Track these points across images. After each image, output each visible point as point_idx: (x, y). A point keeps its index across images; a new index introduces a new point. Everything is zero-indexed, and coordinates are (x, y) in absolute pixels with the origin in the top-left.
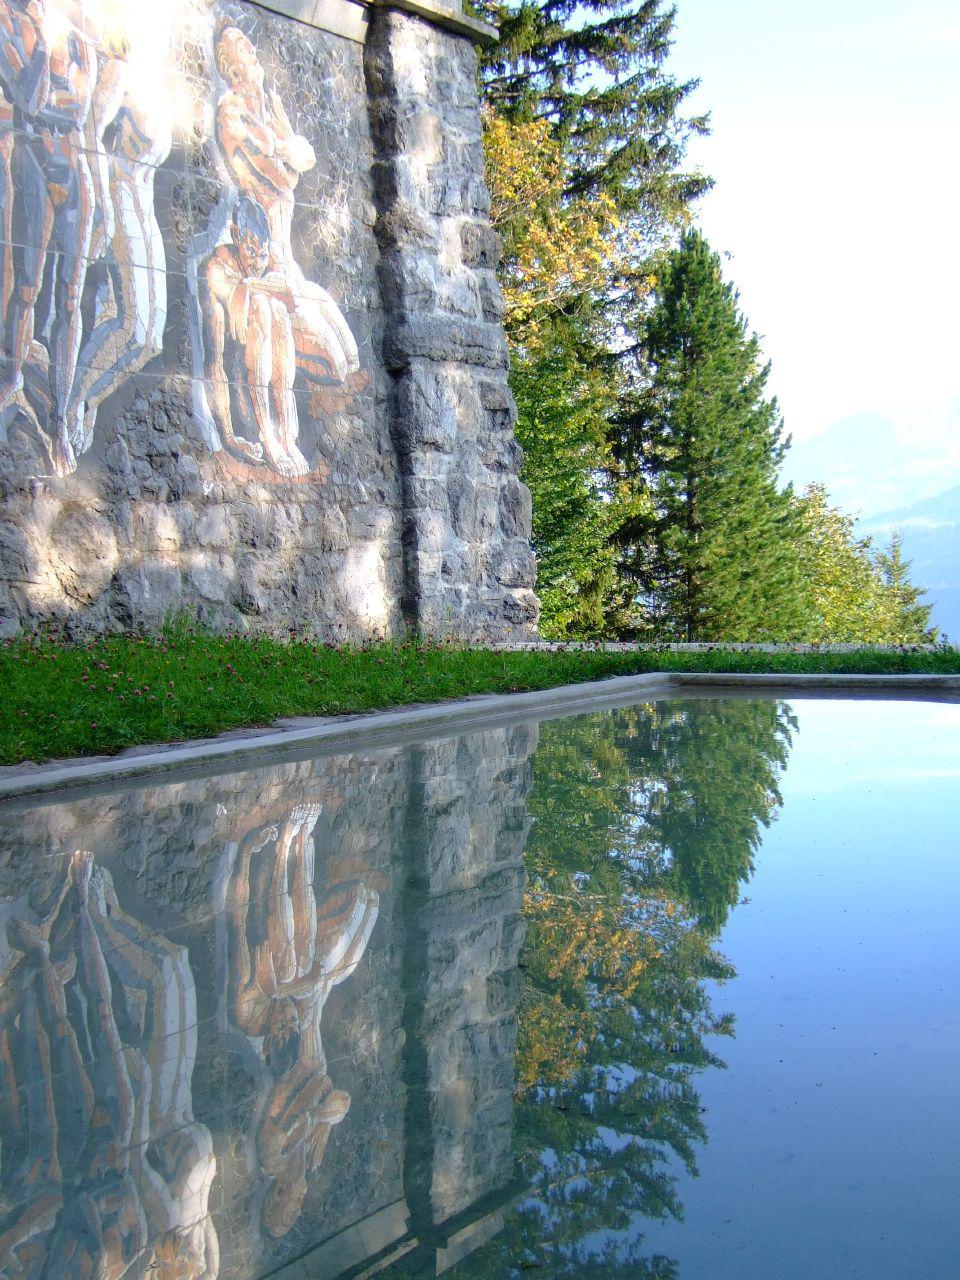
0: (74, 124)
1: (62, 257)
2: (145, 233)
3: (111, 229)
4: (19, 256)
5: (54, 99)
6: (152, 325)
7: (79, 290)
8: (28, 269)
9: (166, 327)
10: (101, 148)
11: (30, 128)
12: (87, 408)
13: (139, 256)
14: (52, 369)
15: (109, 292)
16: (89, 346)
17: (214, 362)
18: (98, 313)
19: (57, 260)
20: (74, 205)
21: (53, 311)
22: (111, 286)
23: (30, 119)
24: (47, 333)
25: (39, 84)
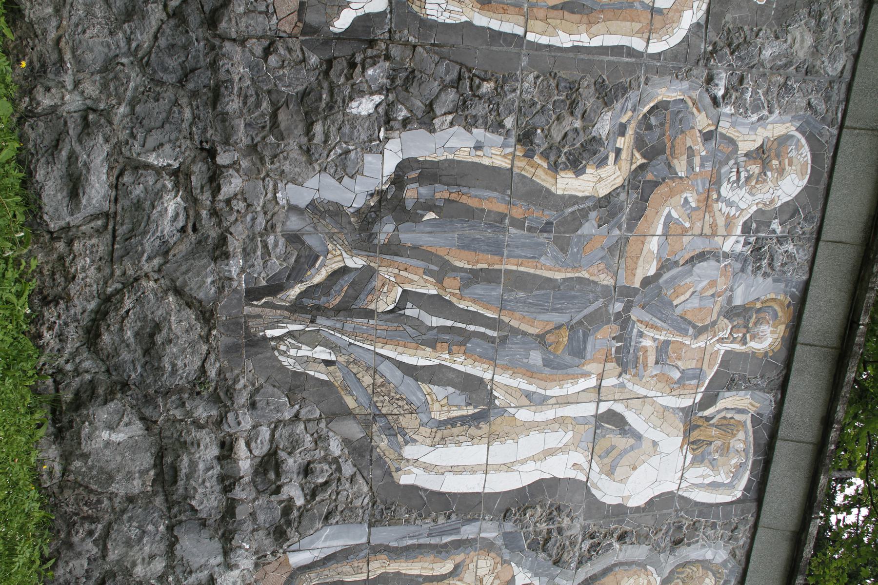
0: (625, 371)
1: (492, 340)
2: (523, 462)
3: (524, 415)
4: (489, 277)
5: (647, 343)
6: (428, 468)
7: (462, 364)
8: (479, 289)
9: (426, 490)
10: (604, 407)
11: (619, 307)
12: (328, 363)
13: (501, 452)
14: (369, 314)
15: (459, 407)
16: (399, 373)
17: (390, 559)
18: (435, 388)
19: (490, 333)
20: (547, 363)
21: (435, 321)
22: (464, 413)
23: (628, 307)
24: (411, 311)
25: (660, 323)
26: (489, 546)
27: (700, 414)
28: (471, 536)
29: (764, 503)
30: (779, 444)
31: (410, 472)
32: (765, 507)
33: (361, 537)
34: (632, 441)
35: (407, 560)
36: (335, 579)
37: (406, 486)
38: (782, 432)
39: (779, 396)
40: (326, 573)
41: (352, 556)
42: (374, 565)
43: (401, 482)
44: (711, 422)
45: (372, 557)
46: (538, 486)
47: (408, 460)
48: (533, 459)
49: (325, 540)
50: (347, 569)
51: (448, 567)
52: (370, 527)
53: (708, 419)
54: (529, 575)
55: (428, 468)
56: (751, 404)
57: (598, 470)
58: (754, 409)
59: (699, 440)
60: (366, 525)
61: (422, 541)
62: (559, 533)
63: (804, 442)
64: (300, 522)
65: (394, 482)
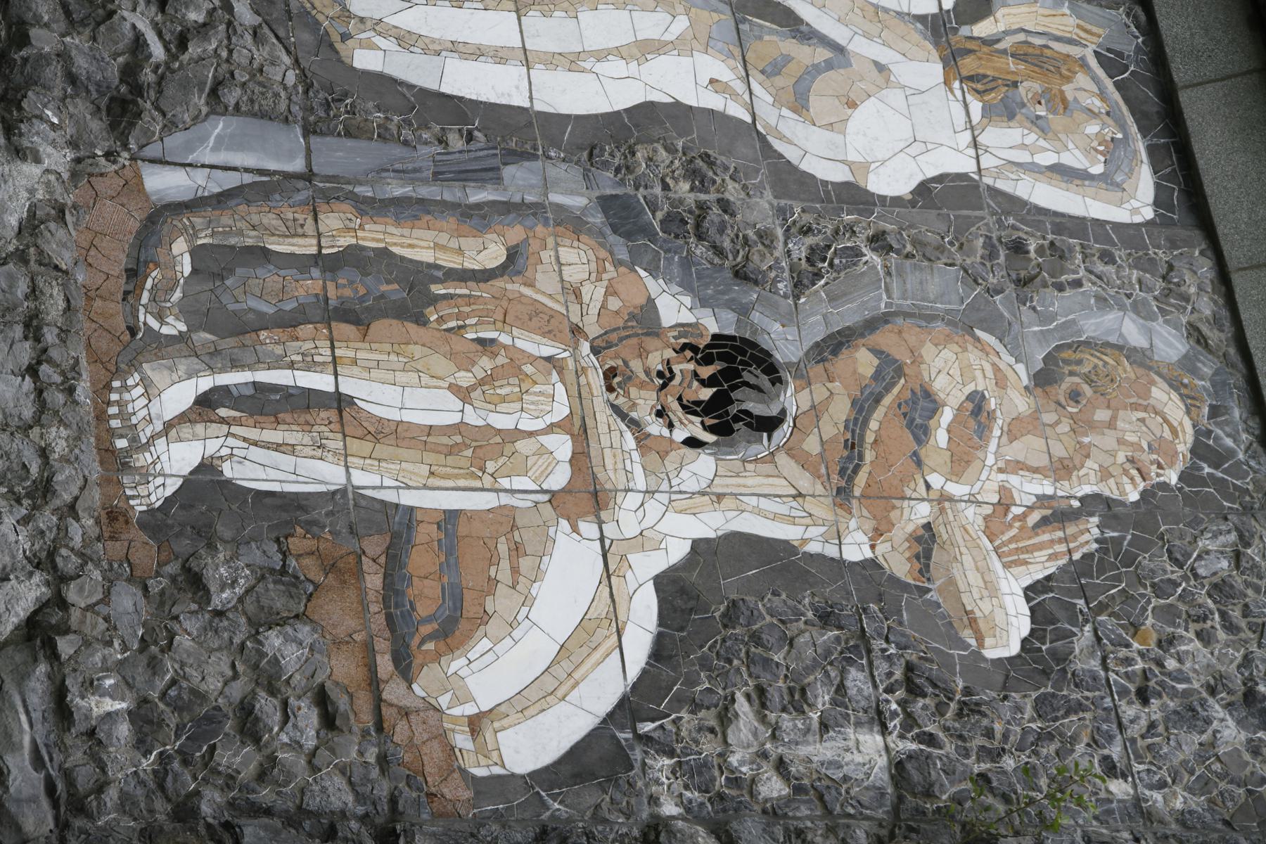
2: (602, 55)
26: (572, 224)
27: (965, 31)
28: (530, 198)
29: (1216, 220)
30: (1184, 97)
31: (373, 47)
32: (1222, 229)
33: (291, 157)
34: (823, 54)
35: (398, 222)
36: (250, 242)
37: (366, 74)
38: (1180, 71)
39: (1143, 17)
40: (226, 220)
41: (277, 197)
42: (331, 221)
43: (357, 64)
44: (1000, 46)
45: (322, 207)
46: (646, 113)
47: (362, 20)
48: (618, 52)
49: (215, 149)
50: (270, 220)
51: (492, 254)
52: (306, 135)
53: (988, 42)
54: (687, 300)
55: (406, 40)
56: (1078, 26)
57: (770, 99)
58: (1095, 39)
59: (985, 76)
60: (299, 131)
61: (424, 192)
62: (725, 211)
63: (1235, 76)
64: (160, 92)
65: (340, 61)
